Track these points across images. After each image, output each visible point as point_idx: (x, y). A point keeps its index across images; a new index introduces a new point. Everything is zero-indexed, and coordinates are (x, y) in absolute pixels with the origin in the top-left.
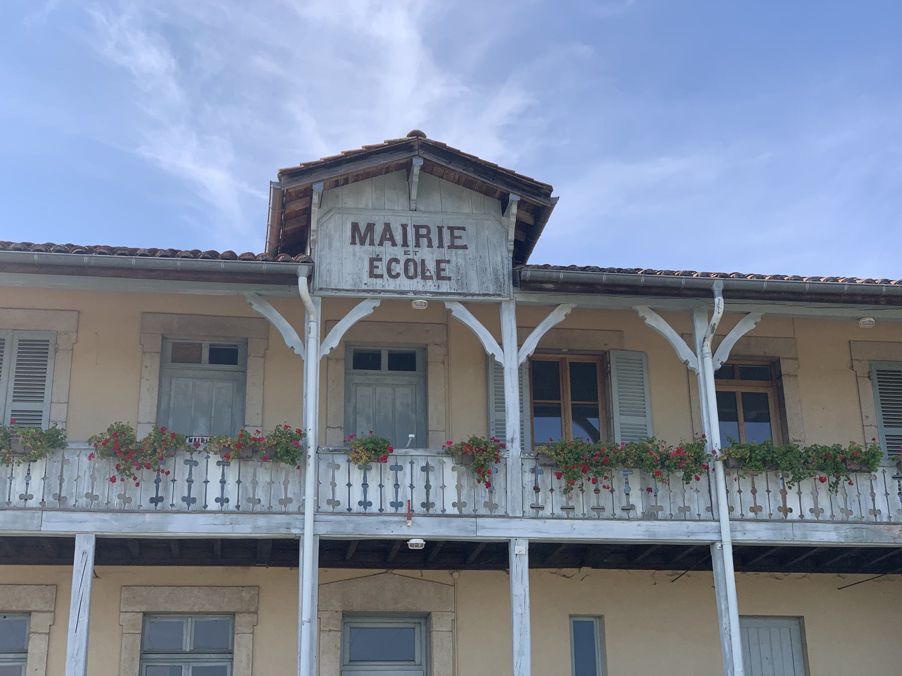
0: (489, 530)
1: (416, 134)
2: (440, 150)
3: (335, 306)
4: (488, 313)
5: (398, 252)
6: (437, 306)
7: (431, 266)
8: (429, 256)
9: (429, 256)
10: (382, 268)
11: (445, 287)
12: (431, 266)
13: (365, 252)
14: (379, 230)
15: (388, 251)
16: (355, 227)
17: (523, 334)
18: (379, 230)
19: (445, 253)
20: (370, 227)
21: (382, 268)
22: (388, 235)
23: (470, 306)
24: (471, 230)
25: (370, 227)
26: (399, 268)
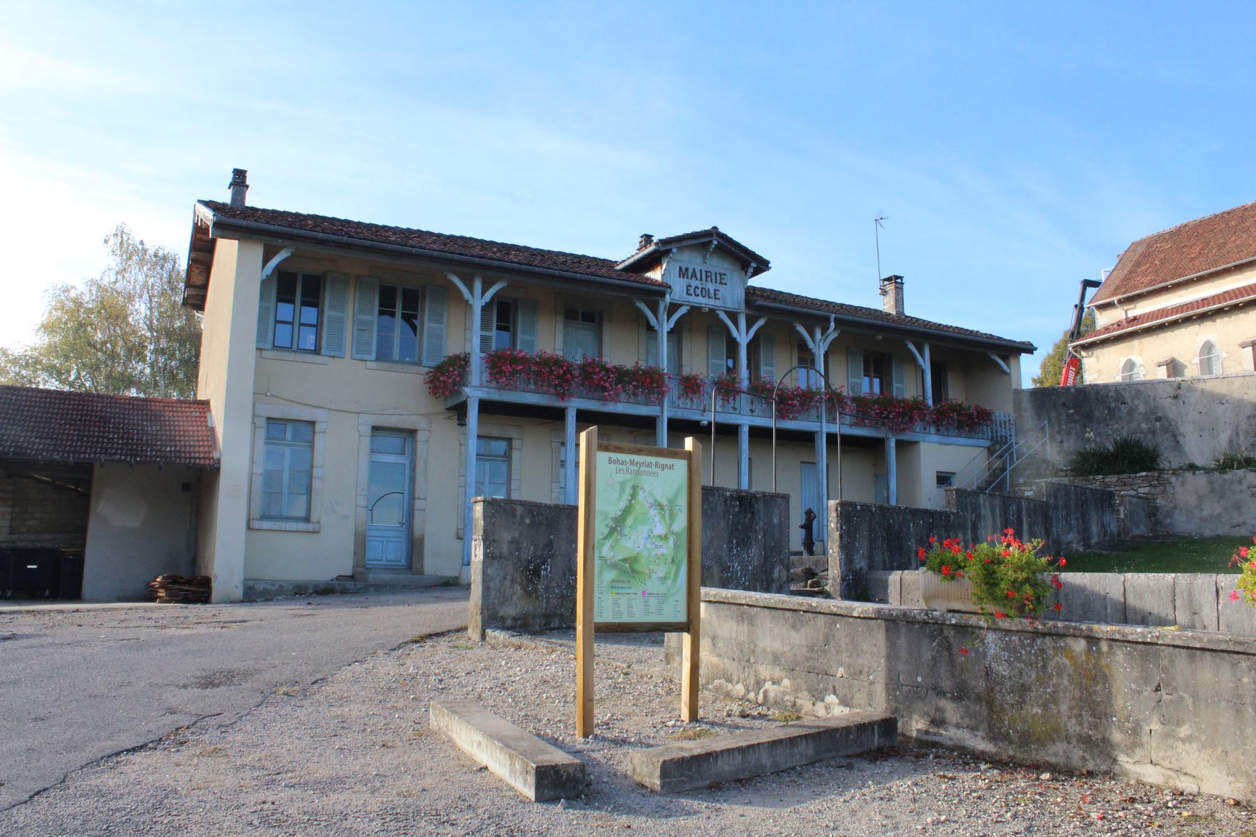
0: (732, 419)
1: (715, 228)
2: (724, 237)
3: (673, 308)
4: (733, 316)
5: (698, 283)
6: (712, 311)
7: (712, 292)
8: (711, 287)
9: (711, 287)
10: (692, 291)
11: (718, 303)
12: (712, 292)
13: (684, 281)
14: (690, 271)
15: (694, 283)
16: (680, 269)
17: (748, 328)
18: (690, 271)
19: (718, 286)
20: (687, 269)
21: (692, 291)
22: (694, 275)
23: (727, 313)
24: (729, 275)
25: (687, 269)
26: (698, 292)
